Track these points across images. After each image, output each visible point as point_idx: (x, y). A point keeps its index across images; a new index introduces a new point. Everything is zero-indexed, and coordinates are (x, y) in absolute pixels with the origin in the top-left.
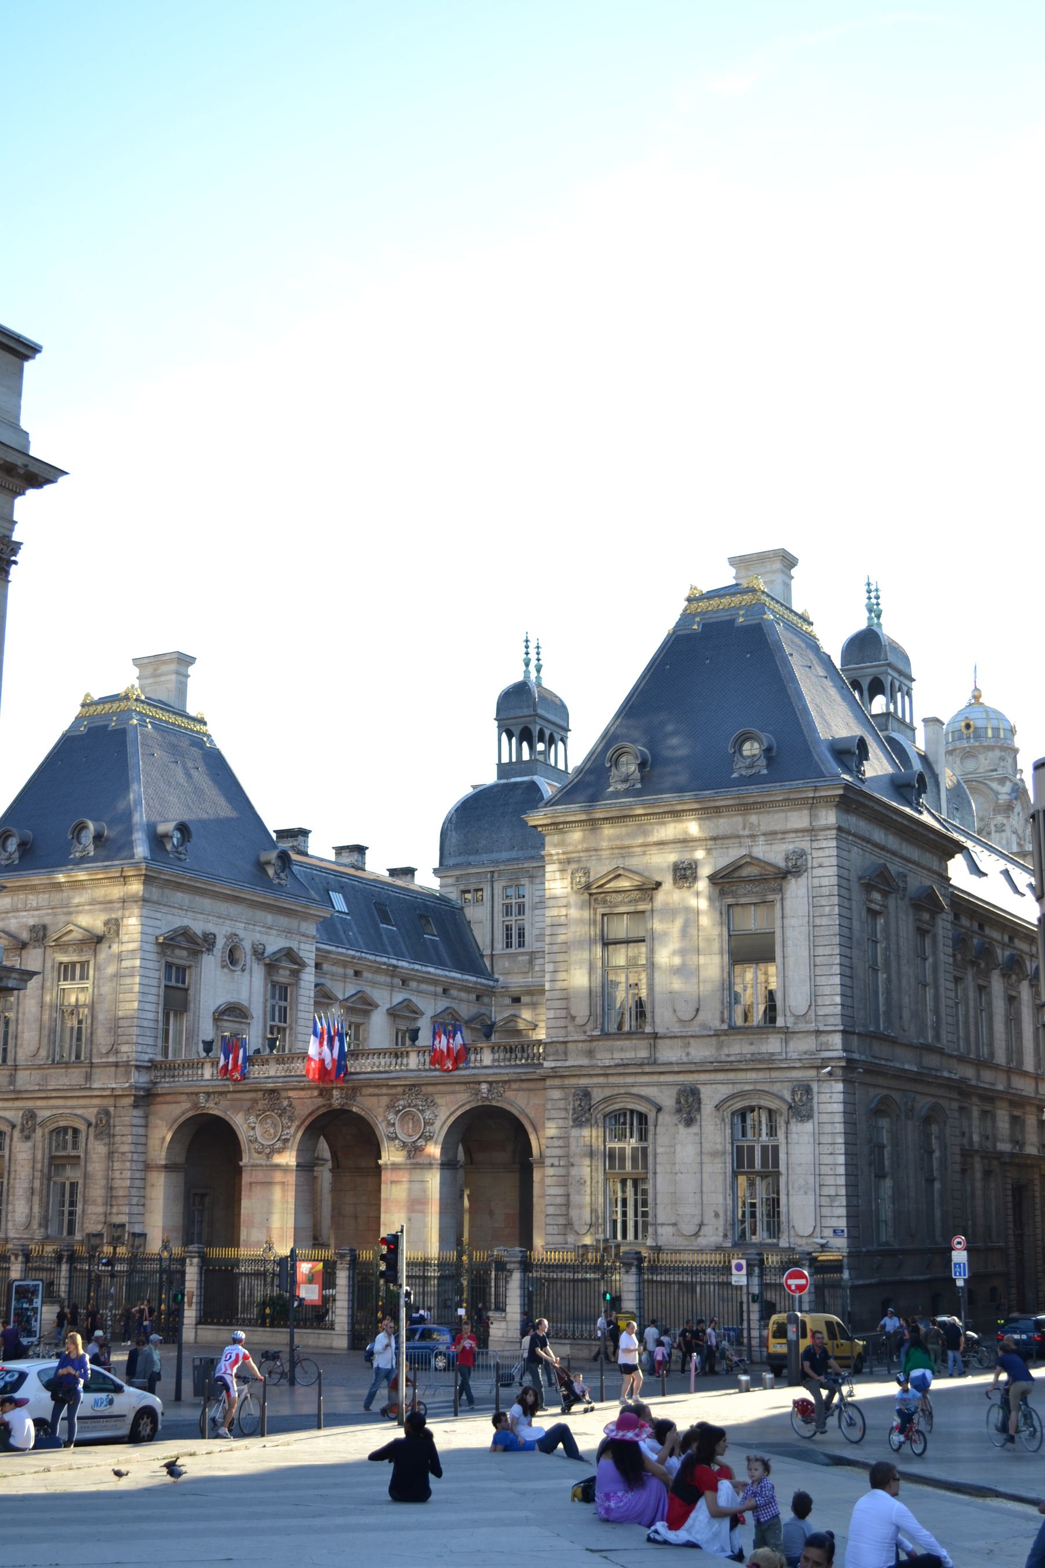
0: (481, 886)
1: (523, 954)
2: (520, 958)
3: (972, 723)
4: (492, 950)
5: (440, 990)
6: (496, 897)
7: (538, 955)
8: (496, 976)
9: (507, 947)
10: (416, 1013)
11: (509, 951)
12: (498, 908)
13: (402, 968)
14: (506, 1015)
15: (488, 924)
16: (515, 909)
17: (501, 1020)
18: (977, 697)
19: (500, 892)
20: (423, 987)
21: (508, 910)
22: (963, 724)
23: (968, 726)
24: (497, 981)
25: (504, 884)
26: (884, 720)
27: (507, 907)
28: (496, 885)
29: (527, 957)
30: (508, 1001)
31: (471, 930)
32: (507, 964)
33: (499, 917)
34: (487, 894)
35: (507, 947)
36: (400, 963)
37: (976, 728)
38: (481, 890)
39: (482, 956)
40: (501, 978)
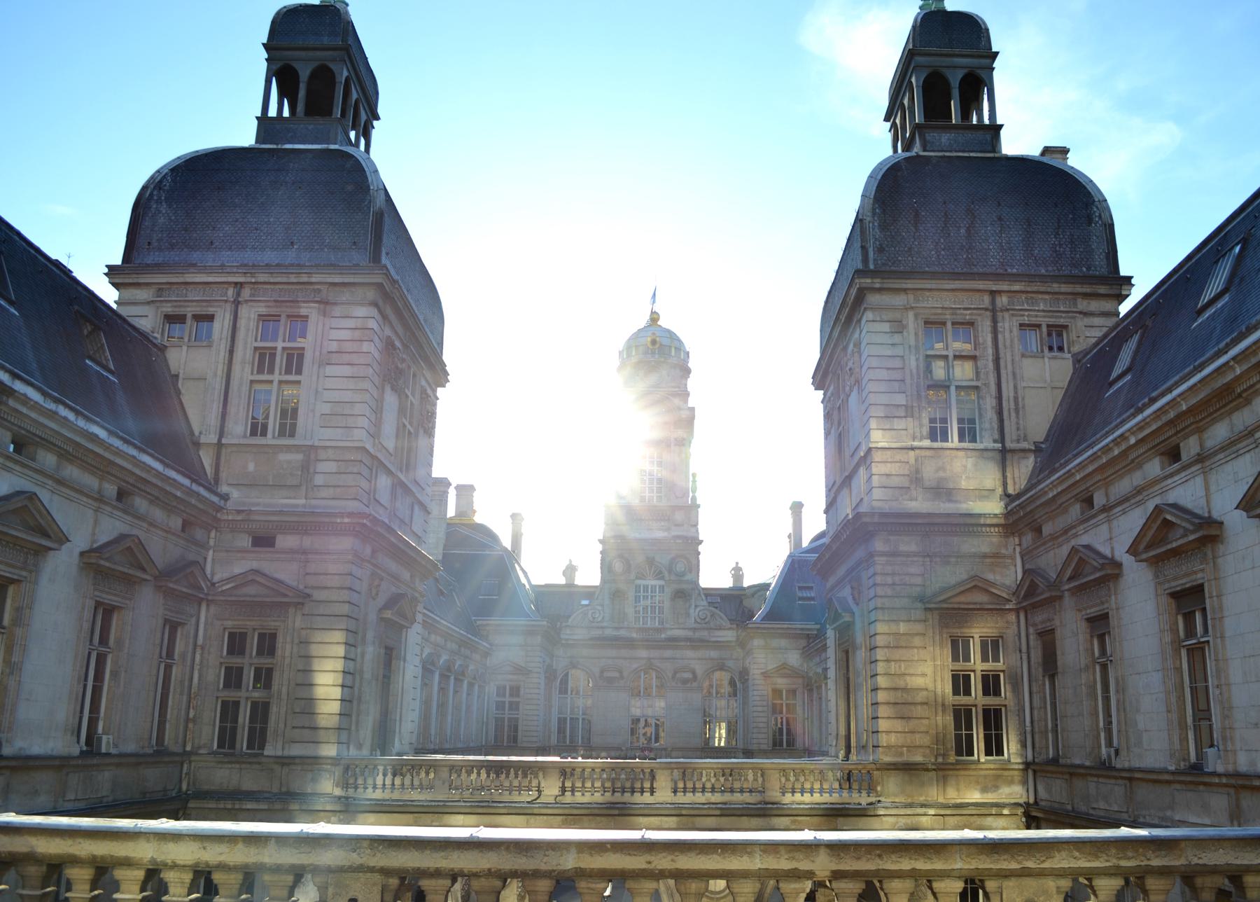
0: (211, 310)
1: (289, 448)
2: (283, 457)
3: (658, 339)
4: (221, 435)
5: (111, 489)
6: (241, 334)
7: (322, 455)
8: (224, 489)
9: (254, 433)
10: (46, 535)
11: (259, 440)
12: (244, 351)
13: (25, 400)
14: (237, 570)
15: (218, 384)
16: (280, 360)
17: (229, 580)
18: (654, 318)
19: (252, 324)
20: (72, 472)
21: (264, 360)
22: (649, 339)
23: (654, 342)
24: (225, 497)
25: (263, 310)
26: (988, 137)
27: (262, 356)
28: (244, 311)
29: (300, 457)
30: (245, 541)
31: (178, 393)
32: (251, 467)
33: (243, 372)
34: (220, 326)
35: (254, 433)
36: (19, 386)
37: (661, 345)
38: (210, 318)
39: (197, 444)
40: (235, 494)
